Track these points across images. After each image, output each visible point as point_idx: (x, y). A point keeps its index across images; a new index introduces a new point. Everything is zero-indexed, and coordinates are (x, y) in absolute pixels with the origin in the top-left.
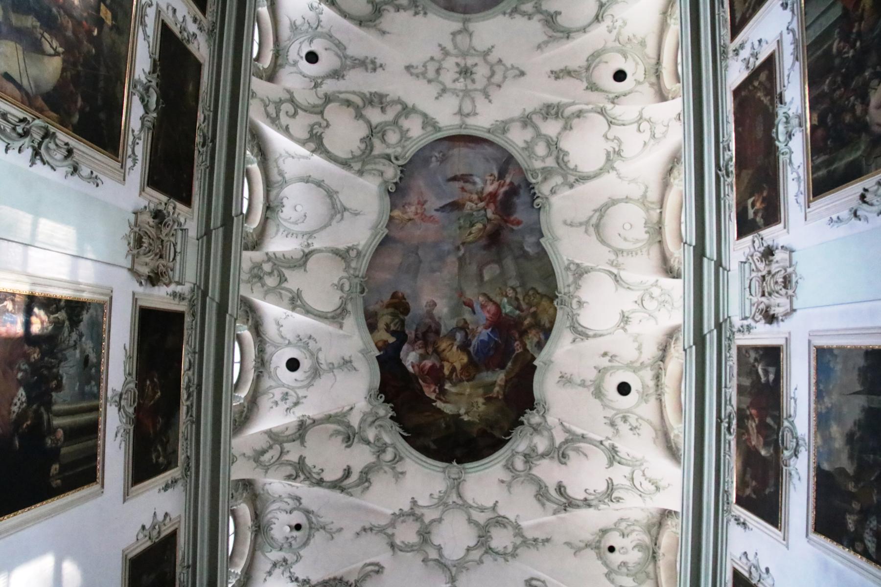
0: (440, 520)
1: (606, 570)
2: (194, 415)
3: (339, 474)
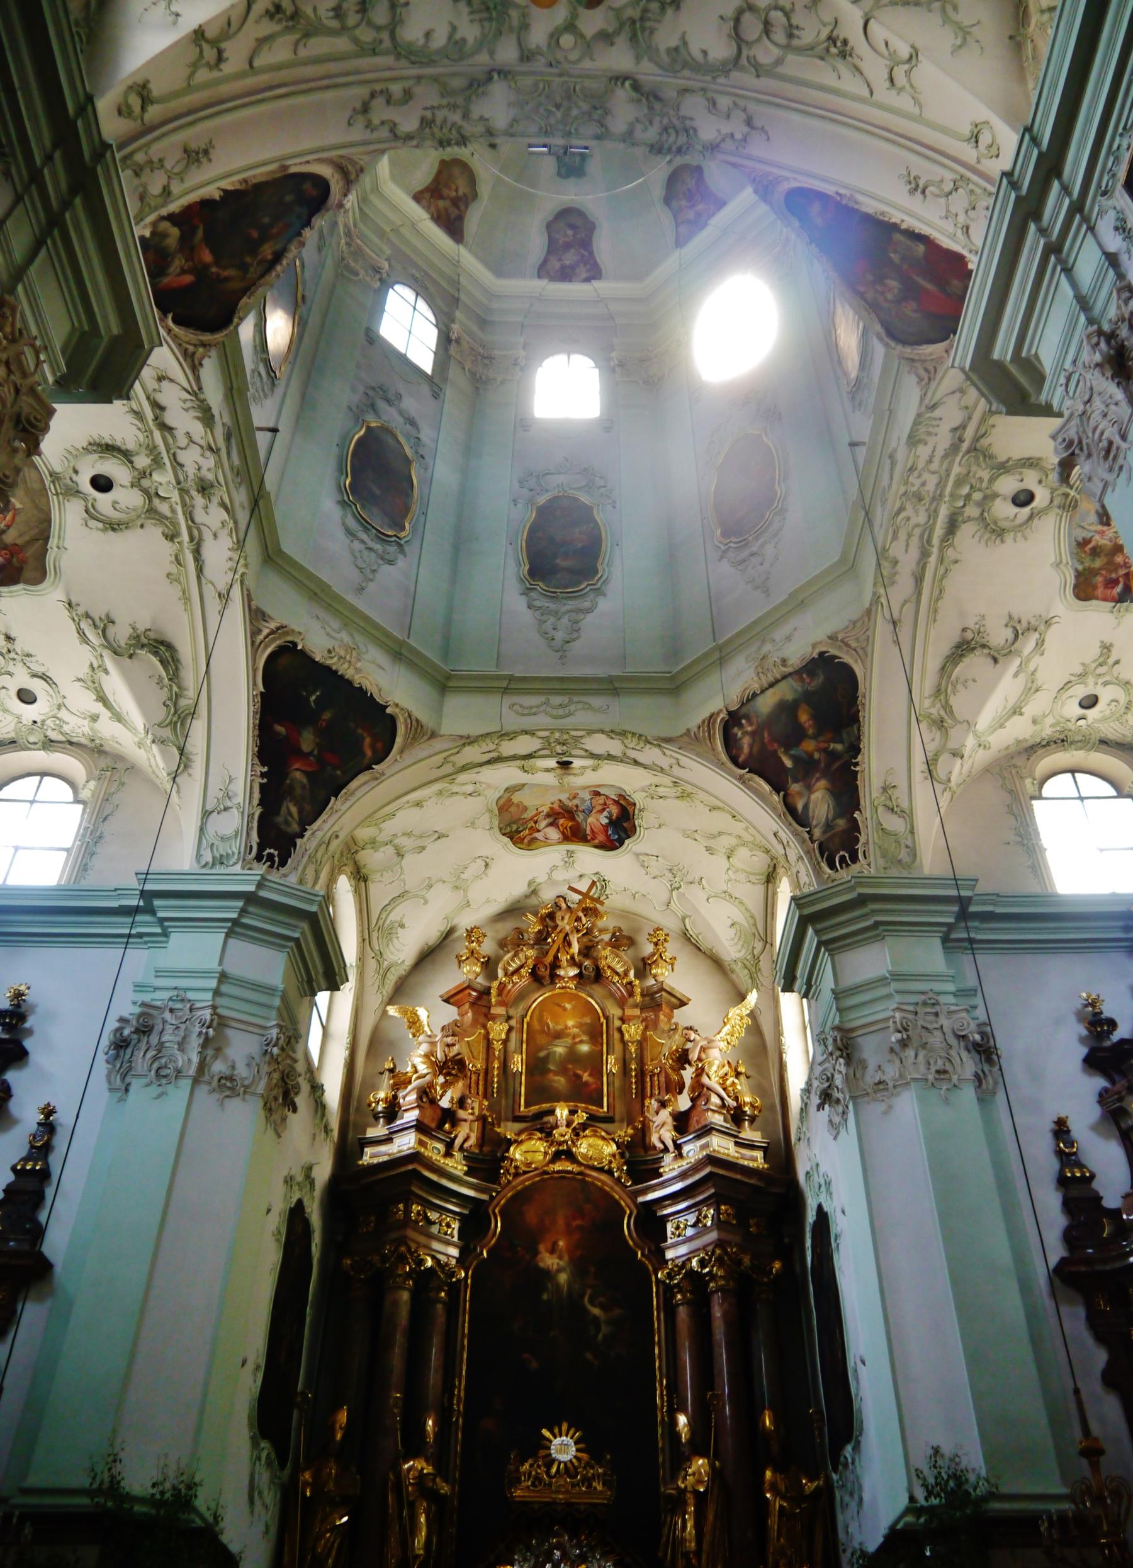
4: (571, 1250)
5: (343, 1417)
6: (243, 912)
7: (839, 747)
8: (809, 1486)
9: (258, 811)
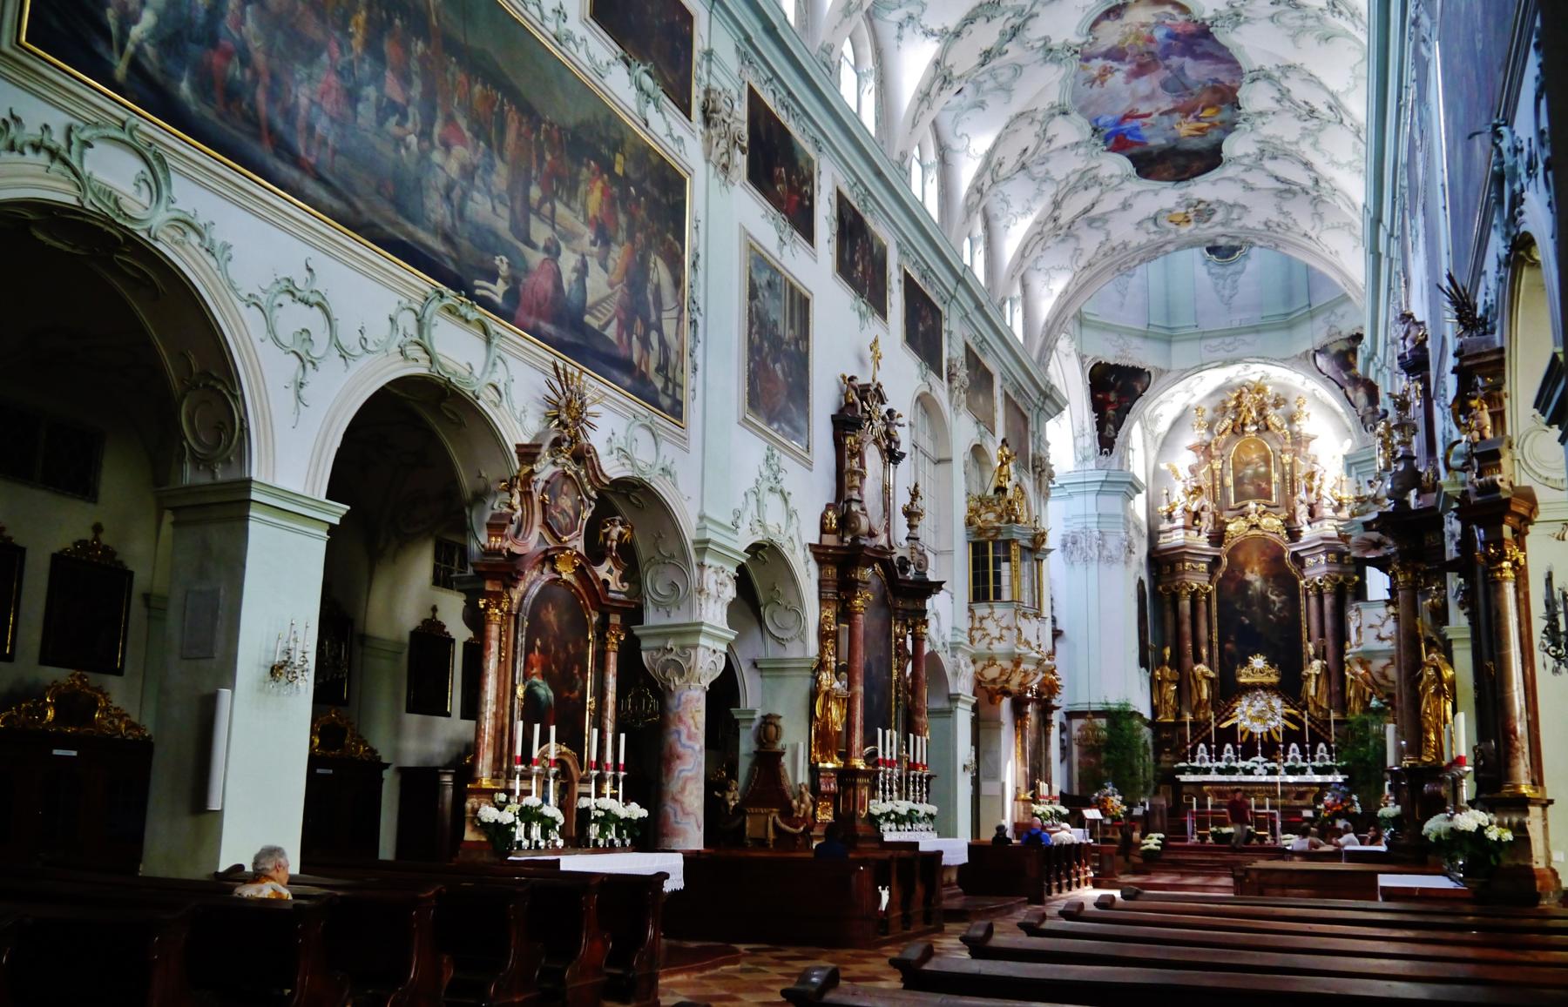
4: (1261, 571)
5: (1168, 651)
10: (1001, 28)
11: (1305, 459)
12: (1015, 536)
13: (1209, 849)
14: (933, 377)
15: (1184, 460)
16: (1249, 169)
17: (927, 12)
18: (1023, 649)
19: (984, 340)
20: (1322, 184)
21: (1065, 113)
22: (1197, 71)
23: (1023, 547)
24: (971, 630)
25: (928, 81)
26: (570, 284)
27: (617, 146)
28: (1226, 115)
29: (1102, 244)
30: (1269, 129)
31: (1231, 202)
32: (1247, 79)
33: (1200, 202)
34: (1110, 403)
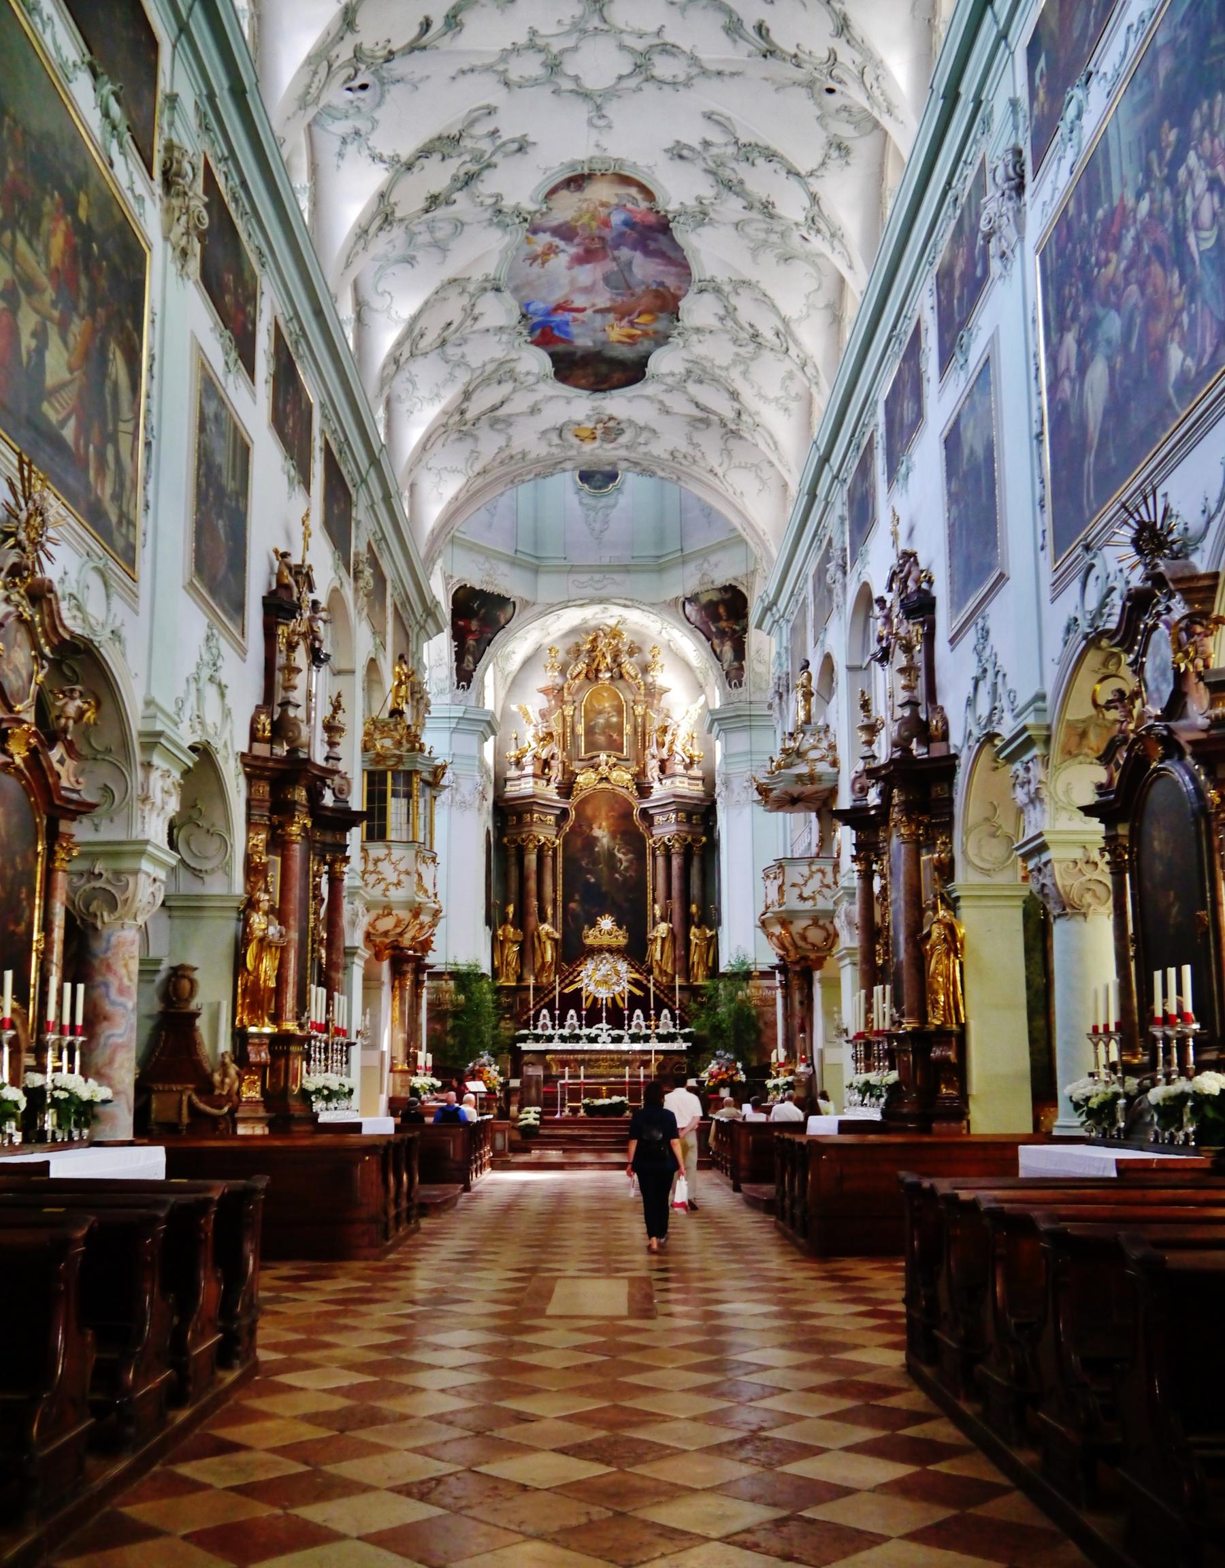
0: (575, 49)
1: (818, 113)
2: (248, 209)
3: (415, 31)
4: (609, 828)
5: (511, 909)
6: (458, 723)
7: (737, 628)
8: (709, 933)
9: (455, 664)
10: (454, 171)
11: (658, 711)
12: (419, 767)
13: (581, 1122)
14: (343, 572)
15: (534, 702)
16: (670, 390)
17: (378, 131)
18: (421, 898)
19: (384, 538)
20: (744, 417)
21: (498, 290)
22: (644, 269)
23: (422, 780)
24: (364, 873)
25: (368, 216)
26: (29, 353)
27: (82, 180)
28: (660, 325)
29: (501, 449)
30: (702, 348)
31: (642, 424)
32: (694, 288)
33: (611, 418)
34: (471, 632)
